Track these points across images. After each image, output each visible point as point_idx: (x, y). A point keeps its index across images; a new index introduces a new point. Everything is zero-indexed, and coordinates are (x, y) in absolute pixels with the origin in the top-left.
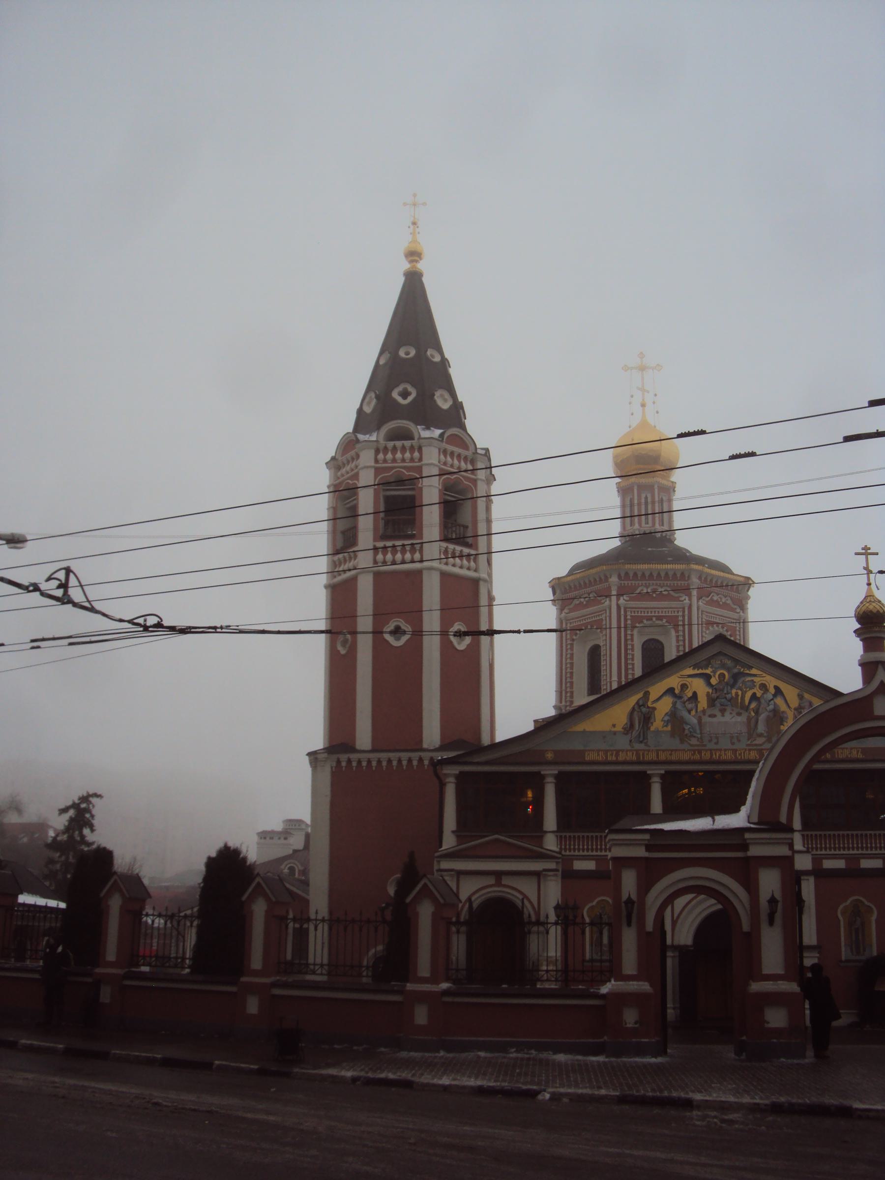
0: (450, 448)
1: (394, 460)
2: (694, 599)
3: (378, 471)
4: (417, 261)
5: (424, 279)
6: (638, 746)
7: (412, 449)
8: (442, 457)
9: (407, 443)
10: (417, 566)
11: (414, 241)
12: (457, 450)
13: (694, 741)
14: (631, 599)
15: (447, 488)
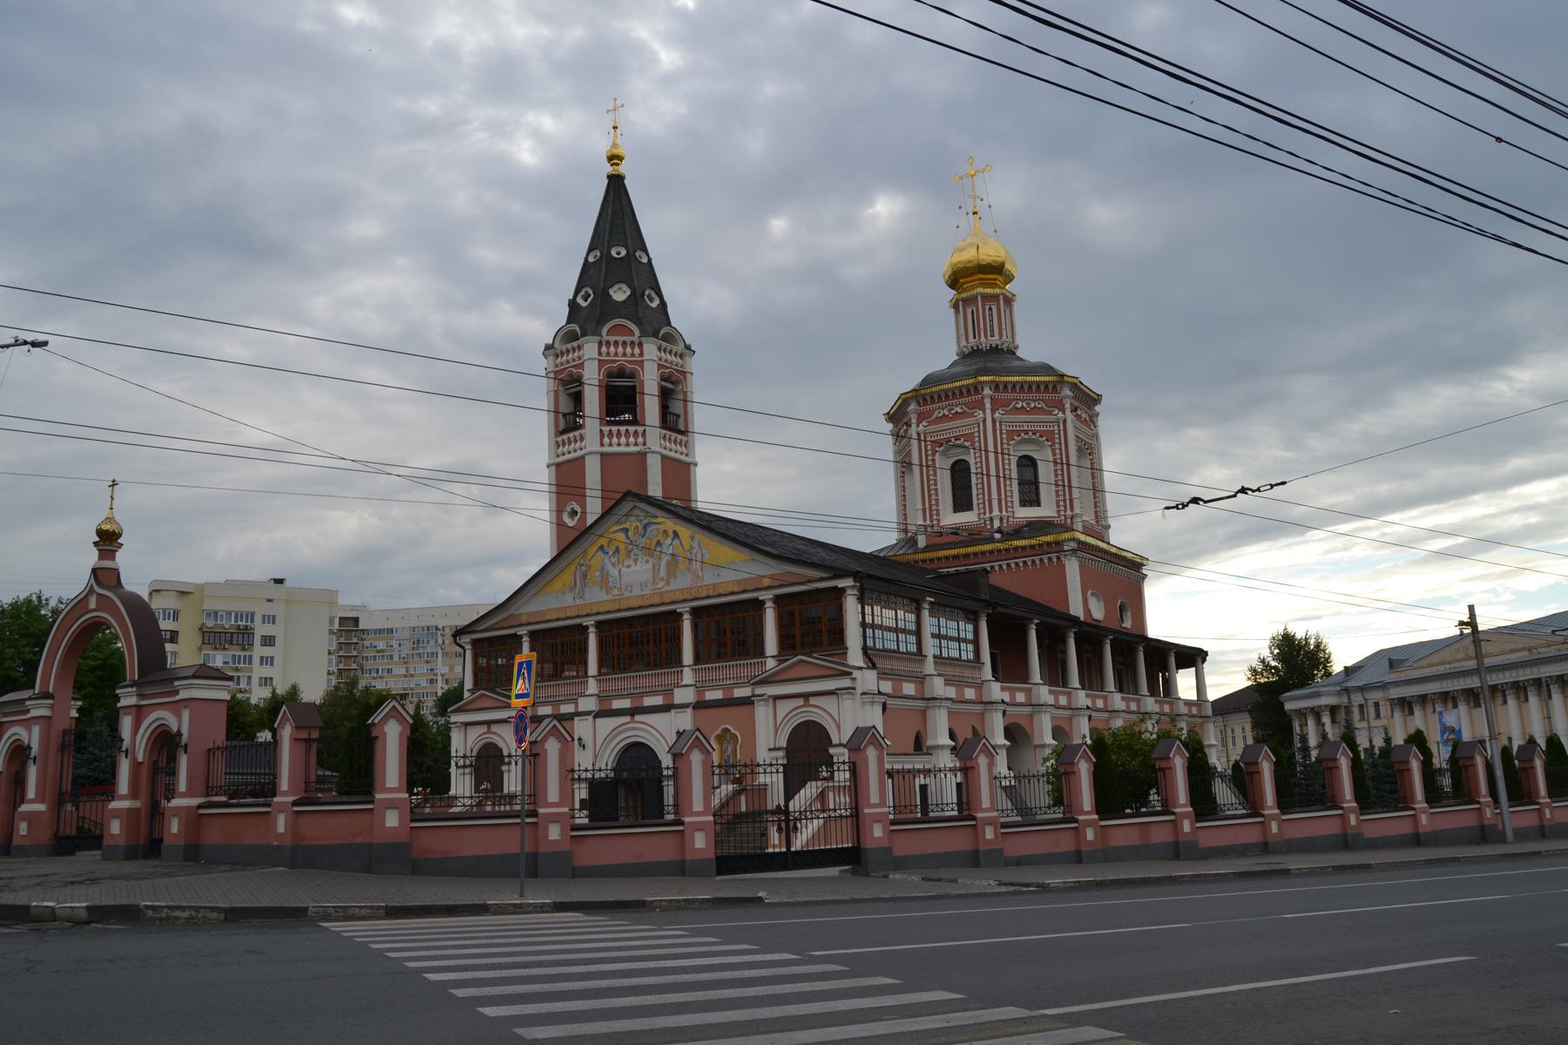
0: (612, 339)
2: (988, 412)
6: (579, 602)
8: (604, 349)
9: (575, 344)
11: (615, 145)
12: (620, 339)
13: (616, 592)
14: (930, 423)
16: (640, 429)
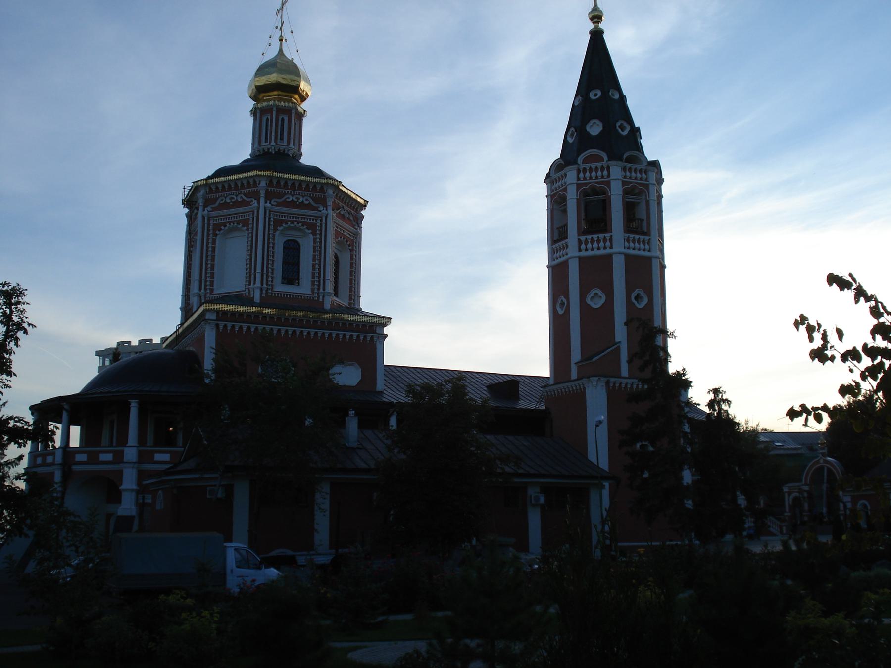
0: (628, 165)
1: (591, 178)
3: (579, 186)
4: (598, 22)
5: (605, 36)
7: (602, 168)
9: (599, 165)
10: (608, 251)
15: (627, 193)
16: (647, 237)
